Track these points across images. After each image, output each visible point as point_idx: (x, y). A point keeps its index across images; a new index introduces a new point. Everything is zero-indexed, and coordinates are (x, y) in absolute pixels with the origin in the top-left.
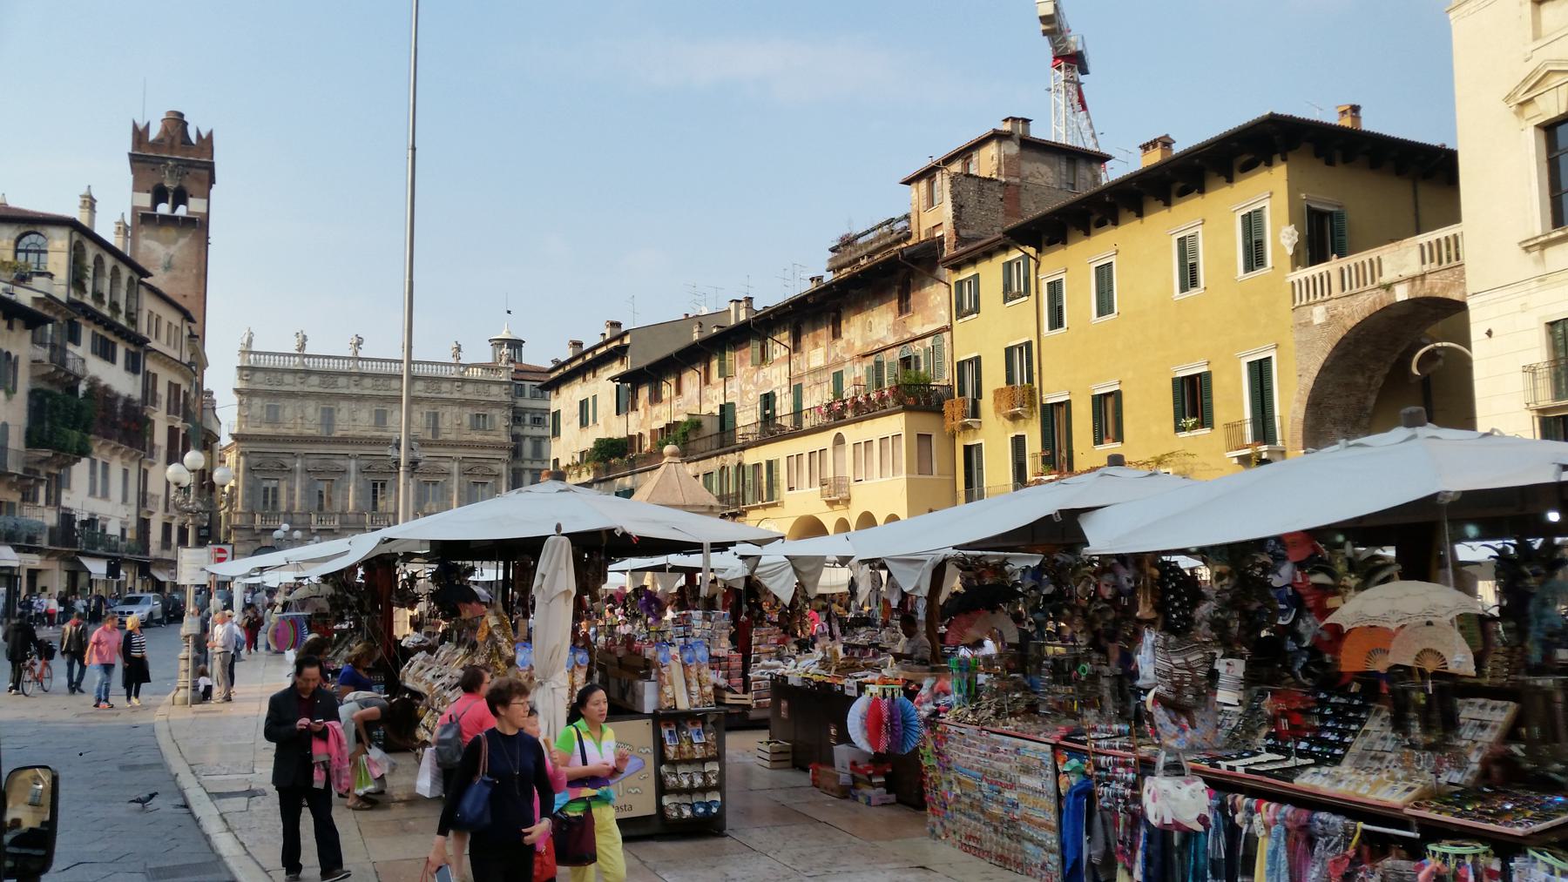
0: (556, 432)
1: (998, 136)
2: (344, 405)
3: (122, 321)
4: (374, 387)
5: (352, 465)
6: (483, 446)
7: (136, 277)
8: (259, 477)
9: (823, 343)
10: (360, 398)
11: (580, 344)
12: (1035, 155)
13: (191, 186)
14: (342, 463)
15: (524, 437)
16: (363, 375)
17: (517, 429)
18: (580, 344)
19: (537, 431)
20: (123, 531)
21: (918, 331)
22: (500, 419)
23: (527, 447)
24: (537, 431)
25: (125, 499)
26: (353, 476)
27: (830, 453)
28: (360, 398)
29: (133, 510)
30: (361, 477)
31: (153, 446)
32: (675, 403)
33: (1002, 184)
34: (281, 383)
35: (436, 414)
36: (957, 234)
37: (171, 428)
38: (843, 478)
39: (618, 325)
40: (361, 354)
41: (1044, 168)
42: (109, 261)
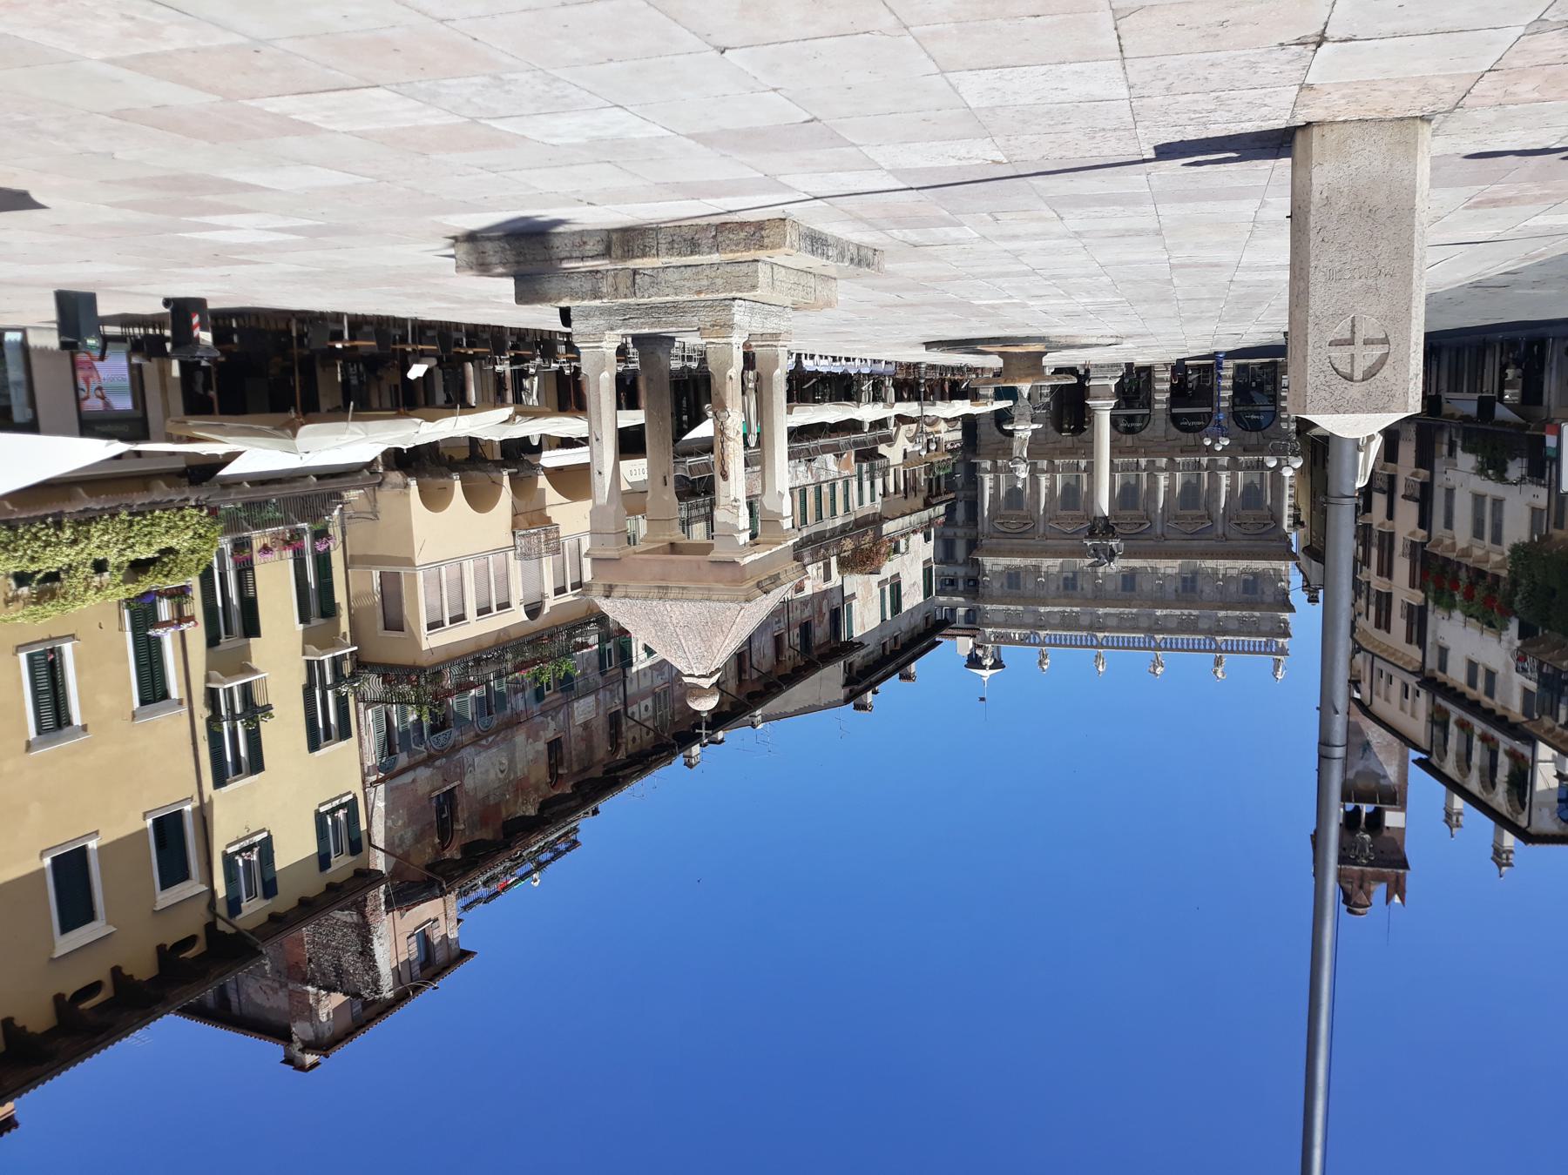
0: (927, 573)
1: (323, 1045)
3: (1455, 713)
7: (1435, 760)
9: (576, 731)
11: (901, 677)
12: (273, 1017)
15: (965, 563)
17: (972, 573)
18: (901, 677)
19: (950, 570)
20: (1451, 452)
21: (423, 773)
23: (960, 550)
24: (950, 570)
25: (1450, 492)
27: (549, 589)
29: (1438, 479)
31: (1412, 556)
32: (782, 625)
33: (311, 981)
36: (363, 916)
37: (1390, 576)
38: (525, 556)
39: (857, 707)
41: (259, 998)
42: (1474, 784)
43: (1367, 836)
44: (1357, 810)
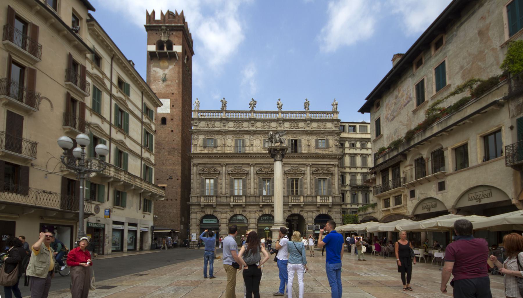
2: (247, 138)
4: (263, 127)
5: (252, 170)
6: (323, 157)
8: (204, 177)
10: (255, 133)
13: (174, 39)
14: (247, 169)
16: (256, 120)
22: (332, 141)
26: (252, 174)
28: (255, 133)
30: (256, 177)
34: (213, 126)
35: (296, 141)
40: (255, 109)
43: (162, 39)
44: (168, 49)
